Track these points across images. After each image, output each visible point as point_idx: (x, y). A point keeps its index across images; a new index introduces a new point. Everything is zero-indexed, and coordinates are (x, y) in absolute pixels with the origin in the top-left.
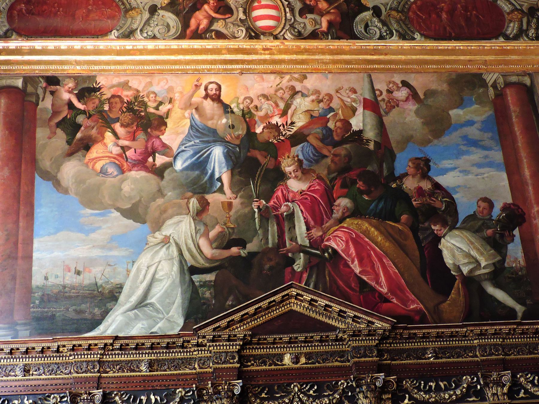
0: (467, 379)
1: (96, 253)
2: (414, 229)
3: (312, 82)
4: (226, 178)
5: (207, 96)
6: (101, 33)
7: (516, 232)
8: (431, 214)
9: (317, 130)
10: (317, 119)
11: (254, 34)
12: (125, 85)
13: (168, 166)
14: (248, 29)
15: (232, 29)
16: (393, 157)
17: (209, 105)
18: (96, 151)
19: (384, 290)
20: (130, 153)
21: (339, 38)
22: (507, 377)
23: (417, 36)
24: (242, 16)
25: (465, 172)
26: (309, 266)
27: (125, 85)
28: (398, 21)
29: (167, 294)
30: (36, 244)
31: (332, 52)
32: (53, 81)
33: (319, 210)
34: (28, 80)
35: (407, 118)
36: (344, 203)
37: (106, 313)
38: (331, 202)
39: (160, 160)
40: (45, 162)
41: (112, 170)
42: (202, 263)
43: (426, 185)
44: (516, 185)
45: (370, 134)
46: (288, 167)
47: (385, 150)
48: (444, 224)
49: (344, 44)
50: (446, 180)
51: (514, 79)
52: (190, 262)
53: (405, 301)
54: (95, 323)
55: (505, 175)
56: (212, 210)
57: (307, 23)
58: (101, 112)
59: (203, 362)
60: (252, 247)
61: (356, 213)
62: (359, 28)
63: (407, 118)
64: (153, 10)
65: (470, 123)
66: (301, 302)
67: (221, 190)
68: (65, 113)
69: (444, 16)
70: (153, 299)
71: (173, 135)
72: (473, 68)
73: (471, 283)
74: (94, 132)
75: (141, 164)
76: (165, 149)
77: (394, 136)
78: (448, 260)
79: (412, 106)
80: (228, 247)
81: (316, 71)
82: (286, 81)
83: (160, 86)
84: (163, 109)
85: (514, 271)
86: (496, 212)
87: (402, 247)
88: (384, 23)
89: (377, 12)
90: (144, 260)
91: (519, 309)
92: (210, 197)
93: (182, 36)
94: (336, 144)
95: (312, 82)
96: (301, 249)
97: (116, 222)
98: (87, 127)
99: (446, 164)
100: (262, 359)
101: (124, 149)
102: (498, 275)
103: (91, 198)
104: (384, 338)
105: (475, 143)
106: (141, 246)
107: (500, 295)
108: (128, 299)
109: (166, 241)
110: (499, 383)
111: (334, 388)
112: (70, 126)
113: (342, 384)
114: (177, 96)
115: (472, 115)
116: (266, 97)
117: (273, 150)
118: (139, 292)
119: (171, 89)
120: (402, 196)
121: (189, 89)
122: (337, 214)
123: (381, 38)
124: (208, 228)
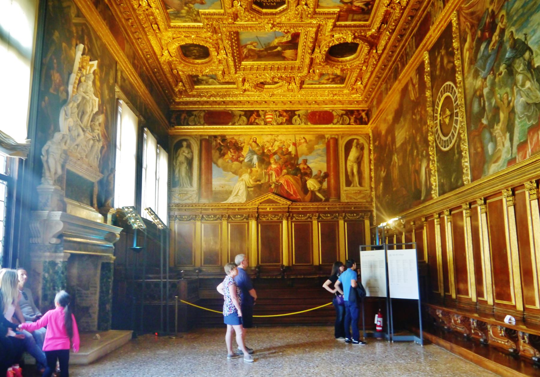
1: (226, 183)
2: (301, 178)
3: (280, 137)
4: (257, 164)
5: (253, 141)
6: (227, 124)
7: (326, 179)
8: (306, 174)
9: (280, 151)
10: (280, 148)
11: (266, 123)
12: (233, 138)
13: (243, 161)
14: (265, 122)
15: (260, 122)
16: (298, 159)
17: (254, 144)
18: (226, 157)
19: (292, 193)
20: (234, 157)
21: (288, 124)
22: (317, 214)
23: (309, 123)
24: (263, 118)
25: (316, 163)
26: (275, 187)
27: (233, 138)
28: (305, 119)
29: (242, 193)
30: (213, 180)
31: (286, 128)
32: (215, 137)
33: (278, 172)
34: (210, 136)
35: (303, 148)
36: (285, 171)
37: (229, 197)
38: (281, 170)
39: (241, 159)
40: (214, 159)
41: (230, 161)
42: (250, 186)
43: (306, 167)
44: (328, 167)
45: (293, 153)
46: (272, 161)
47: (296, 157)
49: (289, 126)
50: (310, 165)
51: (333, 136)
52: (248, 185)
53: (296, 196)
54: (226, 199)
56: (254, 172)
57: (280, 120)
58: (227, 146)
59: (250, 209)
60: (262, 182)
61: (288, 174)
62: (293, 121)
64: (240, 116)
65: (319, 149)
66: (271, 196)
67: (255, 167)
68: (219, 146)
69: (317, 117)
71: (244, 153)
72: (322, 133)
73: (313, 192)
74: (226, 151)
75: (237, 160)
76: (243, 156)
77: (299, 153)
78: (308, 186)
79: (305, 144)
80: (256, 182)
82: (273, 137)
83: (241, 139)
84: (242, 145)
85: (324, 190)
86: (322, 174)
87: (297, 182)
88: (301, 120)
89: (299, 116)
90: (237, 184)
91: (324, 199)
92: (253, 169)
93: (247, 124)
94: (284, 155)
95: (280, 137)
98: (224, 150)
99: (311, 161)
100: (263, 209)
101: (233, 156)
102: (320, 190)
103: (225, 169)
104: (289, 205)
105: (320, 155)
107: (320, 195)
108: (234, 194)
109: (242, 180)
110: (316, 216)
112: (220, 150)
113: (280, 215)
114: (246, 141)
115: (321, 147)
116: (268, 142)
117: (269, 157)
118: (236, 192)
119: (244, 139)
120: (299, 170)
121: (249, 139)
123: (299, 124)
124: (252, 177)
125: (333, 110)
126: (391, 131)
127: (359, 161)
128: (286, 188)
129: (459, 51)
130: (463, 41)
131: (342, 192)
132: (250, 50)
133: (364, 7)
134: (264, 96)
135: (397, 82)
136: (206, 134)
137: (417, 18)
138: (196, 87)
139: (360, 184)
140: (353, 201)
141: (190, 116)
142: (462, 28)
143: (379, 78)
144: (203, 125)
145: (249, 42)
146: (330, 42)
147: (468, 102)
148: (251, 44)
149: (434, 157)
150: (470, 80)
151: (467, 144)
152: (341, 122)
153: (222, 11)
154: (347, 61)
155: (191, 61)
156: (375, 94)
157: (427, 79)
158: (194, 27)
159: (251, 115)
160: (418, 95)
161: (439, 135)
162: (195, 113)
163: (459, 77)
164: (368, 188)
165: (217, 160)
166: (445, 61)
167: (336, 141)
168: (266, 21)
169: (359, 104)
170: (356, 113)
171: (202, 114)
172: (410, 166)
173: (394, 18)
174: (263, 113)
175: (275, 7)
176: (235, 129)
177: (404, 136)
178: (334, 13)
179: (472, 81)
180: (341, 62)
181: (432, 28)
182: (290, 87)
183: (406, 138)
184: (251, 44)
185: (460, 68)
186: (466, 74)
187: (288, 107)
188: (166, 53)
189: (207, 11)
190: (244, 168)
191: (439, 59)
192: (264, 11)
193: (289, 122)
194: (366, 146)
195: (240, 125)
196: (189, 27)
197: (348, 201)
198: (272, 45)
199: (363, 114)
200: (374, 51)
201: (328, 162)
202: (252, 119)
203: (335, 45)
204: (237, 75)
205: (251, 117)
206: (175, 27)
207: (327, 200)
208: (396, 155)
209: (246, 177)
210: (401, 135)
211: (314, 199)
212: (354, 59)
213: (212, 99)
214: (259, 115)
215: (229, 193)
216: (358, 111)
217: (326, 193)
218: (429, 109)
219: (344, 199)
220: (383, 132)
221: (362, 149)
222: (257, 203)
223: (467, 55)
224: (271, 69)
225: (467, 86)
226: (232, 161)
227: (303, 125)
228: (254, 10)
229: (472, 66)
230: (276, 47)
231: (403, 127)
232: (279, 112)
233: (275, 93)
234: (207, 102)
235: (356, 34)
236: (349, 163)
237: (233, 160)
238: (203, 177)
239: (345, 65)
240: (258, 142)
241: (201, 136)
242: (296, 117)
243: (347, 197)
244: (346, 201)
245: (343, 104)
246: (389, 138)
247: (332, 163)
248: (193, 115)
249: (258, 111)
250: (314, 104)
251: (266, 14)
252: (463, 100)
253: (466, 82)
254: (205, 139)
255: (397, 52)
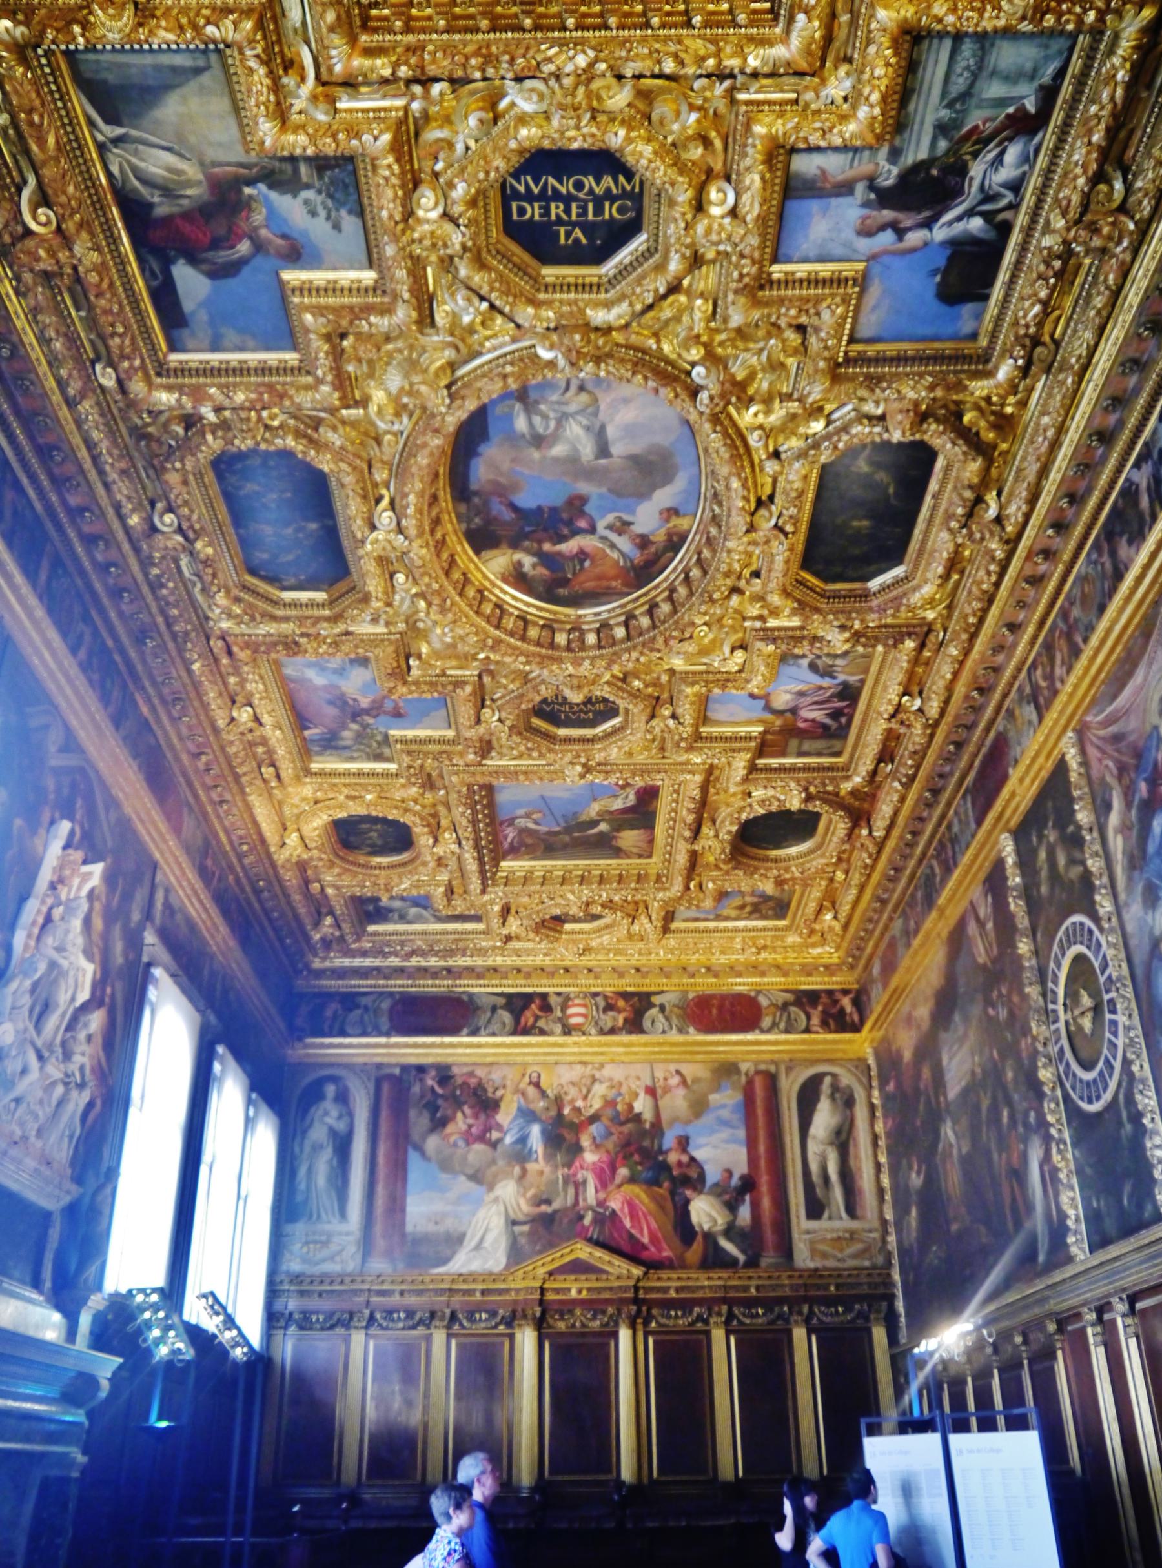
0: (697, 1310)
1: (449, 1208)
2: (673, 1193)
3: (608, 1071)
6: (454, 1031)
7: (748, 1198)
9: (609, 1112)
10: (610, 1103)
11: (567, 1031)
12: (471, 1074)
16: (662, 1134)
17: (531, 1091)
18: (450, 1128)
19: (646, 1240)
21: (630, 1032)
22: (725, 1308)
23: (691, 1030)
26: (595, 1221)
27: (471, 1074)
30: (410, 1200)
31: (624, 1045)
32: (421, 1069)
33: (605, 1178)
34: (405, 1068)
35: (676, 1102)
36: (623, 1172)
37: (454, 1253)
38: (613, 1170)
39: (495, 1135)
40: (415, 1135)
41: (461, 1143)
42: (521, 1217)
43: (685, 1159)
44: (752, 1160)
45: (648, 1116)
46: (585, 1142)
47: (657, 1127)
48: (695, 1189)
49: (634, 1038)
50: (699, 1154)
51: (763, 1067)
52: (512, 1216)
53: (660, 1250)
54: (445, 1261)
55: (744, 1150)
56: (530, 1177)
57: (608, 1020)
59: (517, 1291)
60: (556, 1205)
61: (632, 1180)
62: (646, 1023)
63: (676, 1102)
64: (494, 1009)
65: (724, 1106)
66: (583, 1251)
68: (429, 1096)
70: (487, 1244)
71: (505, 1116)
72: (731, 1057)
73: (709, 1237)
75: (482, 1138)
76: (499, 1127)
77: (665, 1117)
78: (694, 1218)
79: (681, 1092)
81: (612, 1061)
83: (496, 1076)
84: (499, 1093)
85: (742, 1229)
86: (735, 1181)
87: (662, 1207)
89: (662, 1008)
90: (481, 1214)
91: (742, 1258)
93: (514, 1033)
94: (622, 1124)
95: (608, 1071)
96: (590, 1208)
97: (463, 1184)
98: (445, 1108)
99: (702, 1140)
100: (557, 1291)
102: (730, 1231)
103: (445, 1165)
105: (725, 1123)
106: (479, 1203)
108: (470, 1243)
109: (496, 1200)
110: (719, 1314)
111: (604, 1312)
112: (432, 1108)
113: (610, 1310)
115: (727, 1099)
116: (573, 1084)
117: (577, 1128)
120: (665, 1167)
122: (618, 1180)
124: (526, 1190)
125: (759, 992)
126: (928, 1050)
127: (842, 1139)
128: (628, 1223)
129: (1095, 834)
130: (1102, 808)
131: (796, 1235)
132: (523, 831)
133: (828, 721)
134: (565, 953)
135: (934, 914)
136: (393, 1060)
137: (971, 748)
138: (371, 928)
139: (851, 1210)
140: (831, 1263)
141: (350, 1010)
142: (1095, 773)
143: (884, 902)
144: (388, 1034)
145: (521, 812)
146: (742, 809)
147: (1139, 971)
148: (528, 816)
149: (1061, 1130)
150: (1134, 911)
151: (1152, 1093)
152: (782, 1025)
153: (450, 734)
154: (790, 858)
155: (362, 860)
156: (876, 946)
157: (1016, 906)
158: (372, 774)
159: (526, 1007)
160: (995, 951)
161: (1068, 1065)
162: (364, 1001)
163: (1105, 906)
164: (876, 1224)
165: (424, 1138)
166: (1062, 860)
167: (771, 1080)
168: (568, 757)
169: (832, 974)
170: (824, 999)
171: (386, 1005)
172: (995, 1156)
173: (911, 748)
174: (559, 999)
175: (593, 724)
176: (479, 1046)
177: (967, 1067)
178: (748, 738)
179: (1141, 913)
180: (776, 860)
181: (1014, 774)
182: (636, 928)
183: (973, 1073)
184: (528, 816)
185: (1105, 880)
186: (1122, 896)
187: (629, 984)
188: (293, 839)
189: (410, 733)
190: (501, 1163)
191: (1043, 855)
192: (562, 732)
193: (635, 1025)
194: (860, 1094)
195: (493, 1034)
196: (360, 774)
197: (816, 1263)
198: (584, 818)
199: (846, 1002)
200: (865, 832)
201: (751, 1143)
202: (528, 1017)
203: (756, 819)
204: (486, 898)
205: (525, 1011)
206: (321, 773)
207: (752, 1263)
208: (949, 1123)
209: (507, 1189)
210: (959, 1064)
211: (714, 1259)
212: (811, 851)
213: (414, 961)
214: (546, 1008)
215: (455, 1241)
216: (830, 993)
217: (749, 1238)
218: (1033, 991)
219: (803, 1258)
220: (907, 1055)
221: (849, 1103)
222: (541, 1271)
223: (1117, 844)
224: (582, 880)
225: (1130, 927)
226: (468, 1143)
227: (674, 1036)
228: (536, 731)
229: (1136, 874)
230: (594, 823)
231: (962, 1040)
232: (606, 997)
233: (593, 944)
234: (400, 971)
235: (812, 789)
236: (813, 1148)
237: (469, 1138)
238: (381, 1190)
239: (787, 870)
240: (543, 1085)
241: (379, 1066)
242: (654, 1011)
243: (814, 1252)
244: (811, 1265)
245: (786, 975)
246: (926, 1073)
247: (762, 1148)
248: (358, 1006)
249: (544, 996)
250: (702, 976)
251: (568, 740)
252: (1124, 965)
253: (1126, 917)
254: (390, 1077)
255: (928, 833)
